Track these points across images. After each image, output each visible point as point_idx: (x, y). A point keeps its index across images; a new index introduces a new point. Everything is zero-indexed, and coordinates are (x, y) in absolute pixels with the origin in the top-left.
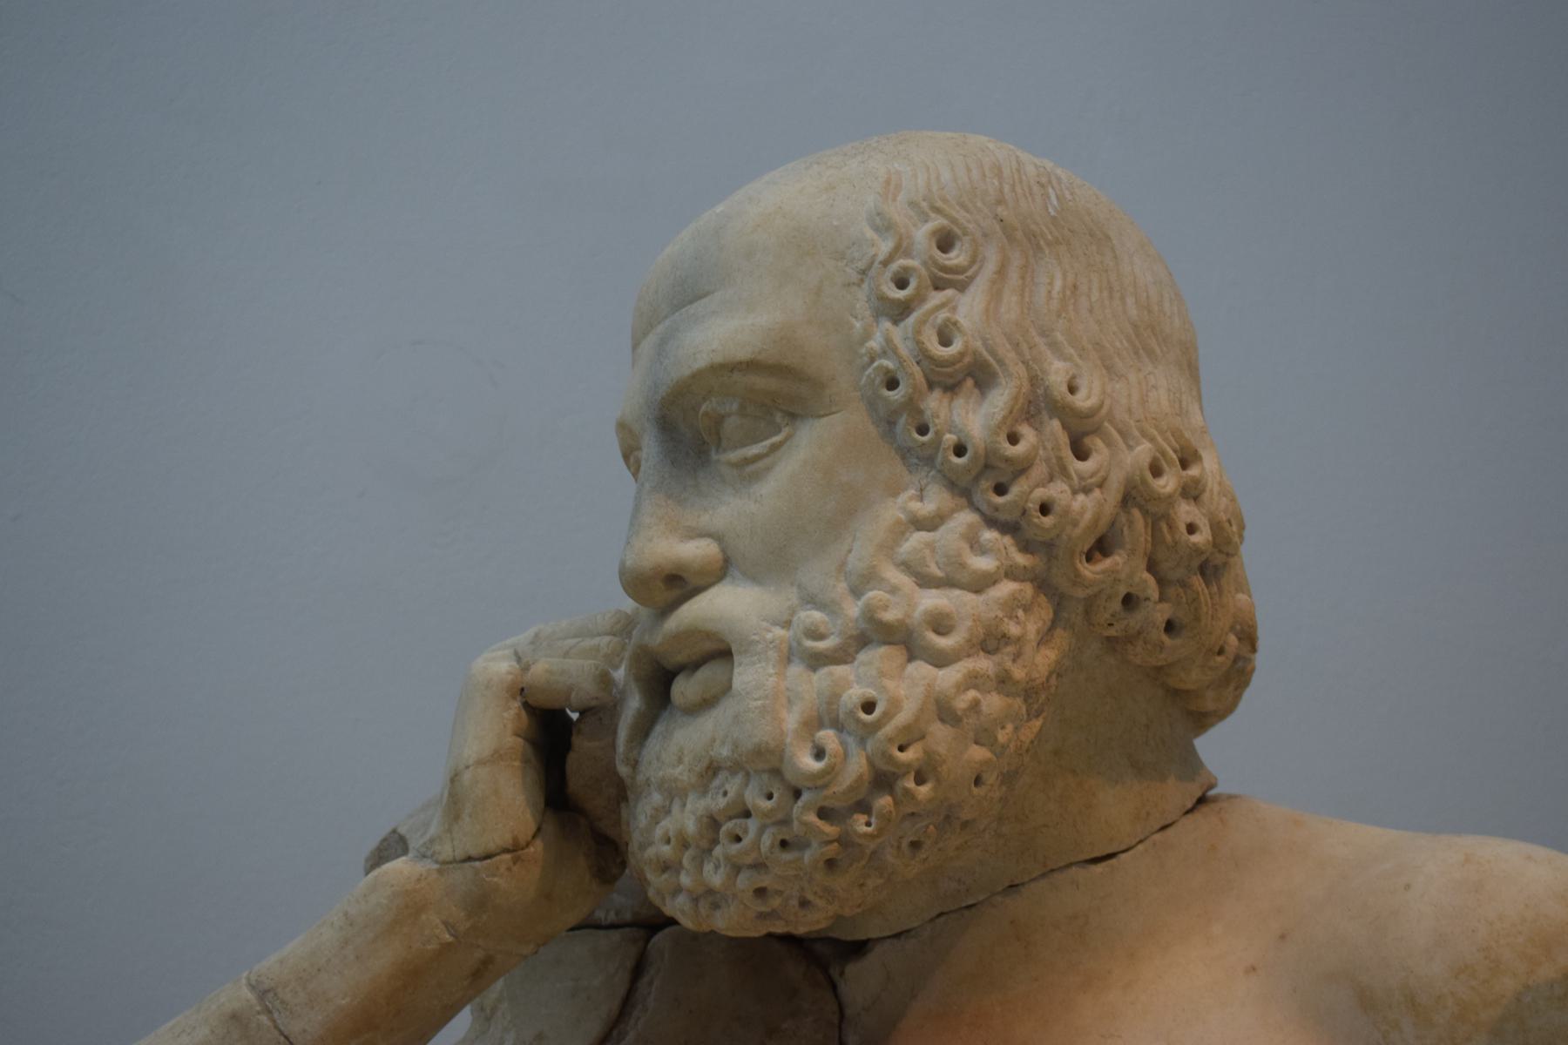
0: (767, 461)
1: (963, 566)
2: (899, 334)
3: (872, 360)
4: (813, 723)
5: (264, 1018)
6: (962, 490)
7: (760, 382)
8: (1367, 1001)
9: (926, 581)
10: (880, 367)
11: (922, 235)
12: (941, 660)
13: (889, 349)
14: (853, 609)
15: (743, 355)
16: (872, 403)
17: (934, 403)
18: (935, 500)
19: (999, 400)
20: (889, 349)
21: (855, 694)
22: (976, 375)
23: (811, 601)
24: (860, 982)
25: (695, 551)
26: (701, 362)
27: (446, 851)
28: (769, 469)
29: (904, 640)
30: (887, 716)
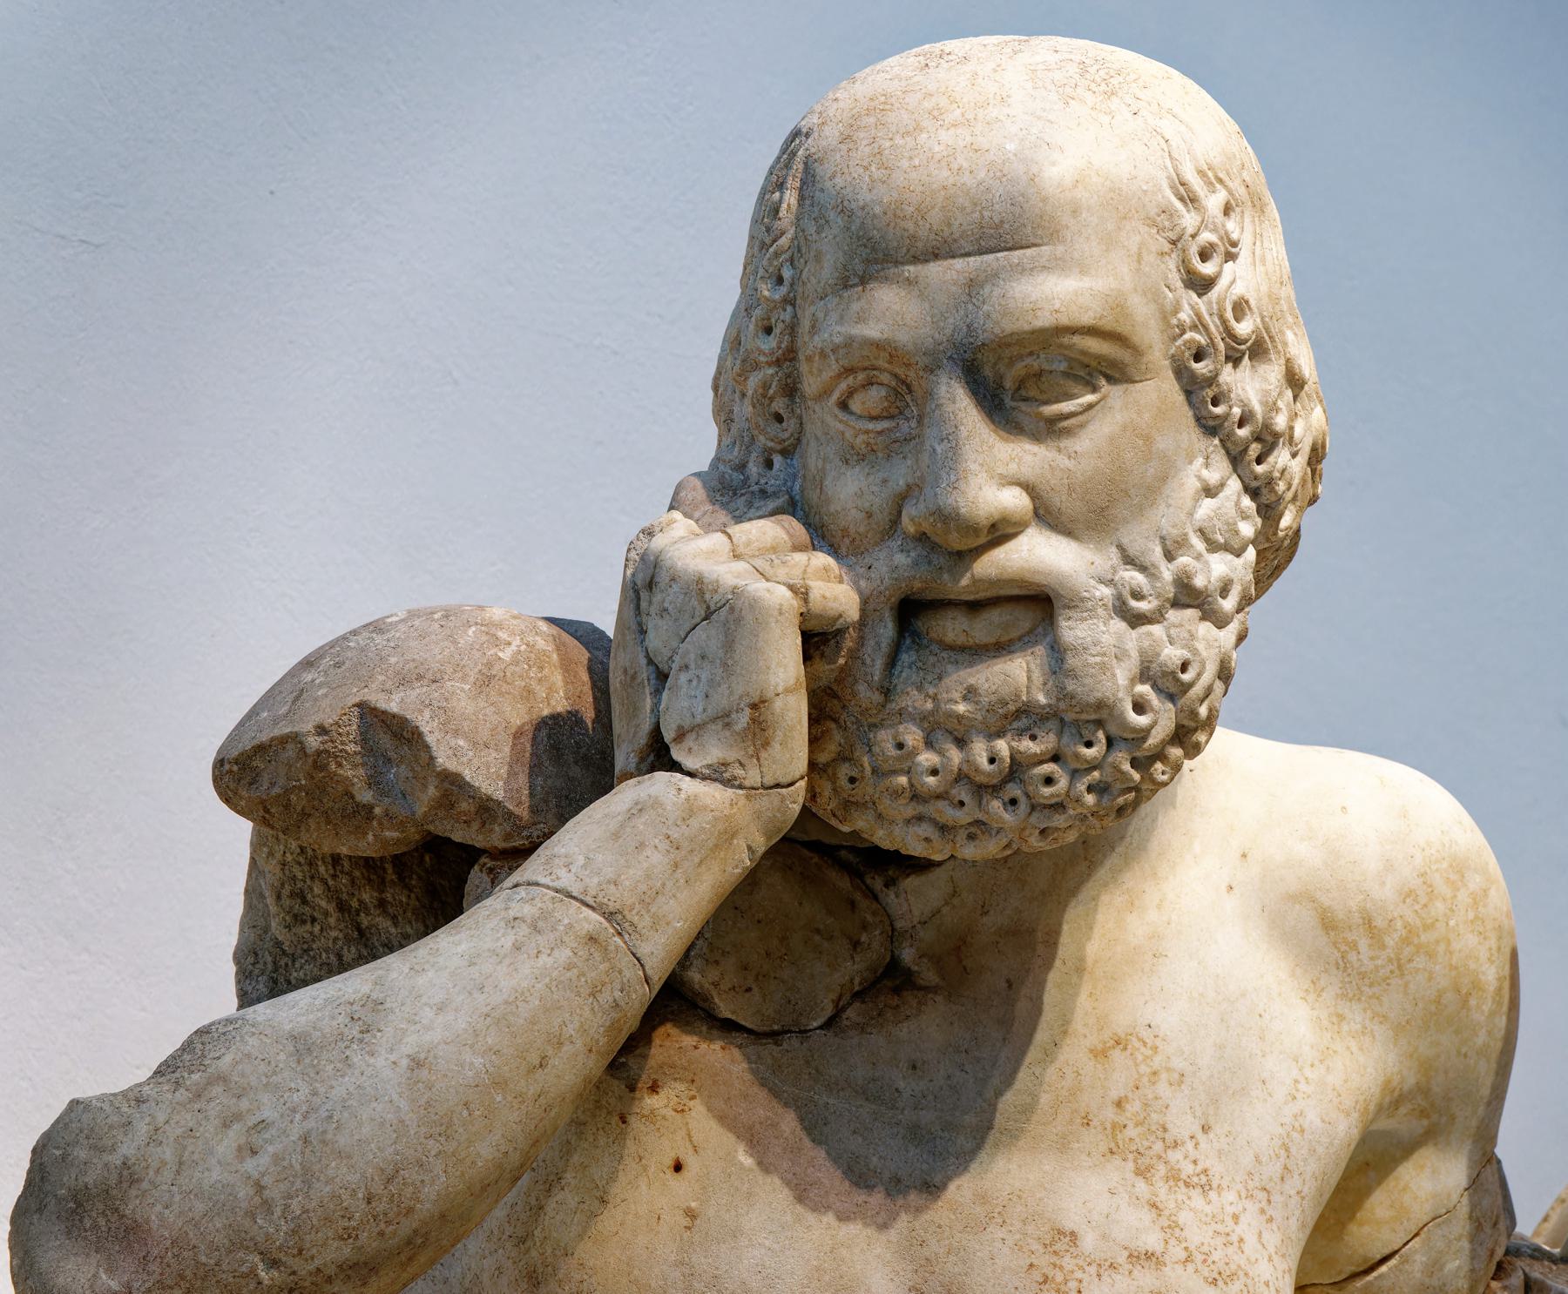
0: (1080, 418)
1: (1237, 532)
2: (1201, 304)
3: (1183, 332)
4: (1133, 682)
5: (617, 939)
6: (1236, 459)
7: (1094, 345)
8: (1328, 923)
9: (1213, 547)
10: (1192, 341)
11: (1214, 202)
12: (1221, 622)
13: (1199, 325)
14: (1167, 573)
15: (1086, 319)
17: (1227, 375)
18: (1218, 470)
19: (1272, 373)
20: (1199, 325)
21: (1172, 654)
22: (1258, 350)
23: (1129, 560)
24: (913, 901)
25: (1013, 500)
26: (1044, 320)
27: (753, 777)
28: (1082, 426)
29: (1187, 595)
30: (1199, 675)
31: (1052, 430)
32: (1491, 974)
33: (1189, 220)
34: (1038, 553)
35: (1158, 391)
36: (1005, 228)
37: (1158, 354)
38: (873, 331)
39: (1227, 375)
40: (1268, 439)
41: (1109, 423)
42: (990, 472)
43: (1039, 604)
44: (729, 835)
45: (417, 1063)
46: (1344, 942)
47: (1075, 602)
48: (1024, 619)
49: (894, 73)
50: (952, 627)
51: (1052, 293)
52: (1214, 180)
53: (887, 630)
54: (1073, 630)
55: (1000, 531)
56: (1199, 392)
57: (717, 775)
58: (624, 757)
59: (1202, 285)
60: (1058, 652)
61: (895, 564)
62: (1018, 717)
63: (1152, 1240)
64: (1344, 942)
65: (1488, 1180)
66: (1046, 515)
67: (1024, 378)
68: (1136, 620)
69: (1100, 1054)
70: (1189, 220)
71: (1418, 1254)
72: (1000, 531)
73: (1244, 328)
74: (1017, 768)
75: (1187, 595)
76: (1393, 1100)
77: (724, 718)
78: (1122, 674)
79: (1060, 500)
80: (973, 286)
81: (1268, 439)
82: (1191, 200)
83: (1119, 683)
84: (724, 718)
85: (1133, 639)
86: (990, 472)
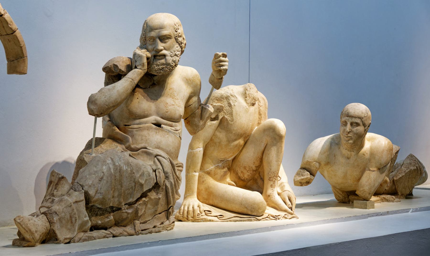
6: (179, 45)
8: (187, 80)
11: (177, 25)
12: (178, 57)
14: (174, 53)
16: (175, 38)
17: (179, 38)
18: (178, 45)
19: (182, 38)
21: (175, 59)
22: (181, 36)
24: (155, 78)
25: (162, 48)
26: (165, 34)
27: (143, 69)
29: (176, 55)
31: (165, 43)
32: (199, 83)
33: (175, 27)
34: (164, 52)
35: (173, 40)
36: (161, 28)
37: (173, 37)
38: (152, 35)
39: (179, 38)
40: (182, 43)
41: (170, 42)
42: (161, 46)
43: (164, 56)
44: (141, 73)
45: (118, 91)
46: (188, 81)
47: (167, 56)
48: (163, 57)
49: (153, 16)
50: (158, 57)
51: (165, 32)
52: (177, 23)
53: (153, 58)
54: (167, 58)
55: (161, 50)
56: (176, 39)
57: (140, 69)
58: (133, 68)
59: (176, 32)
60: (166, 59)
61: (154, 53)
62: (163, 64)
63: (174, 104)
64: (188, 81)
65: (199, 99)
66: (165, 49)
67: (163, 39)
68: (172, 57)
69: (169, 90)
70: (175, 27)
71: (194, 105)
72: (161, 50)
73: (180, 35)
74: (163, 68)
75: (176, 55)
76: (192, 93)
77: (141, 65)
78: (171, 61)
79: (166, 48)
80: (159, 32)
81: (182, 43)
82: (176, 25)
83: (170, 62)
84: (141, 65)
85: (172, 58)
86: (161, 46)
